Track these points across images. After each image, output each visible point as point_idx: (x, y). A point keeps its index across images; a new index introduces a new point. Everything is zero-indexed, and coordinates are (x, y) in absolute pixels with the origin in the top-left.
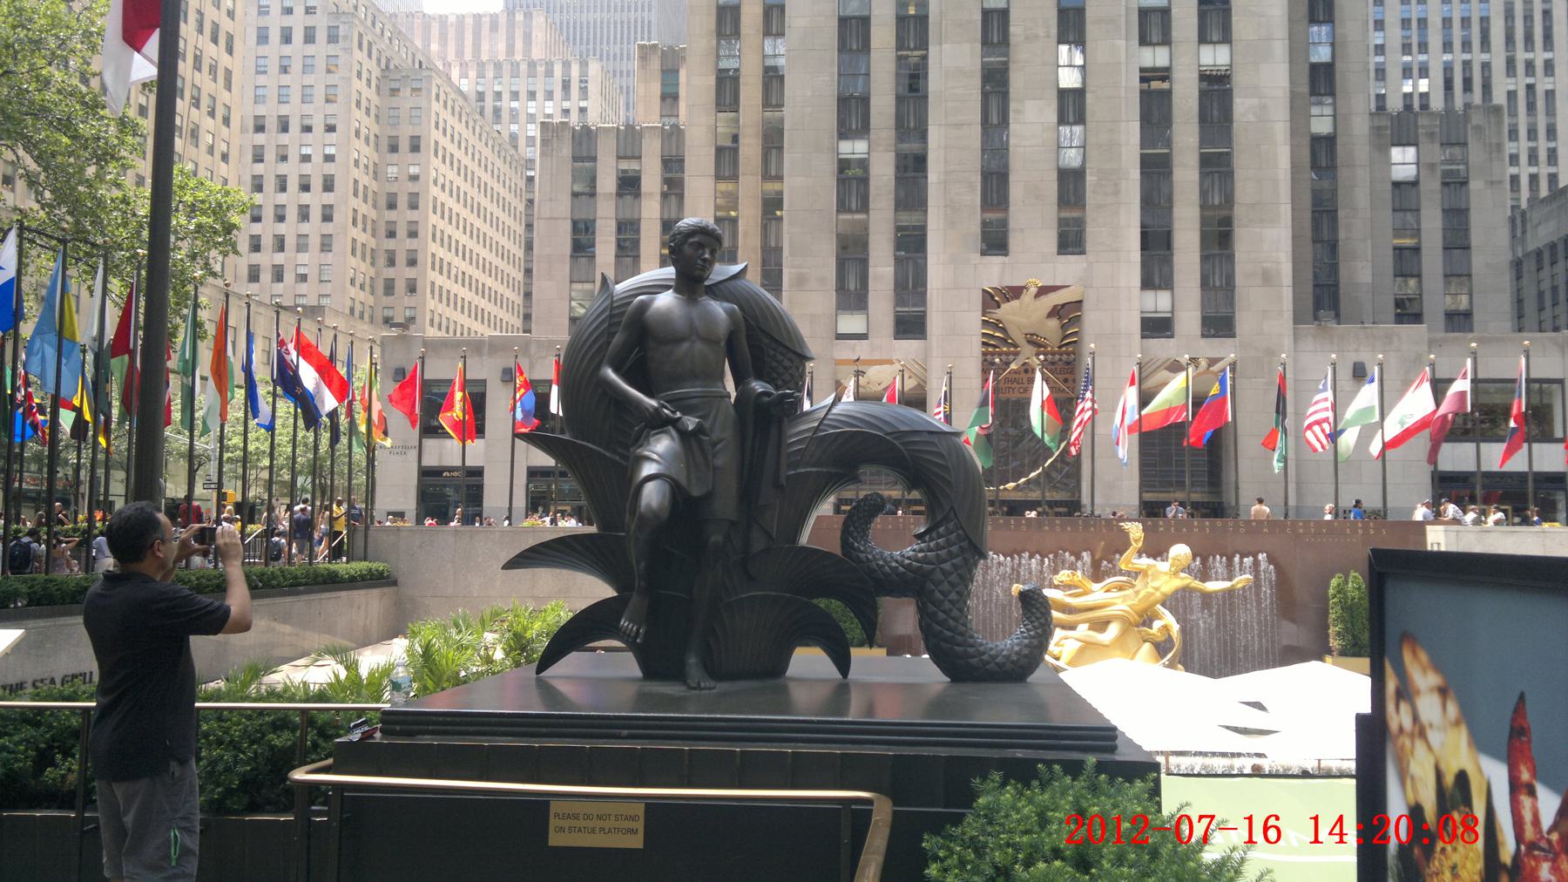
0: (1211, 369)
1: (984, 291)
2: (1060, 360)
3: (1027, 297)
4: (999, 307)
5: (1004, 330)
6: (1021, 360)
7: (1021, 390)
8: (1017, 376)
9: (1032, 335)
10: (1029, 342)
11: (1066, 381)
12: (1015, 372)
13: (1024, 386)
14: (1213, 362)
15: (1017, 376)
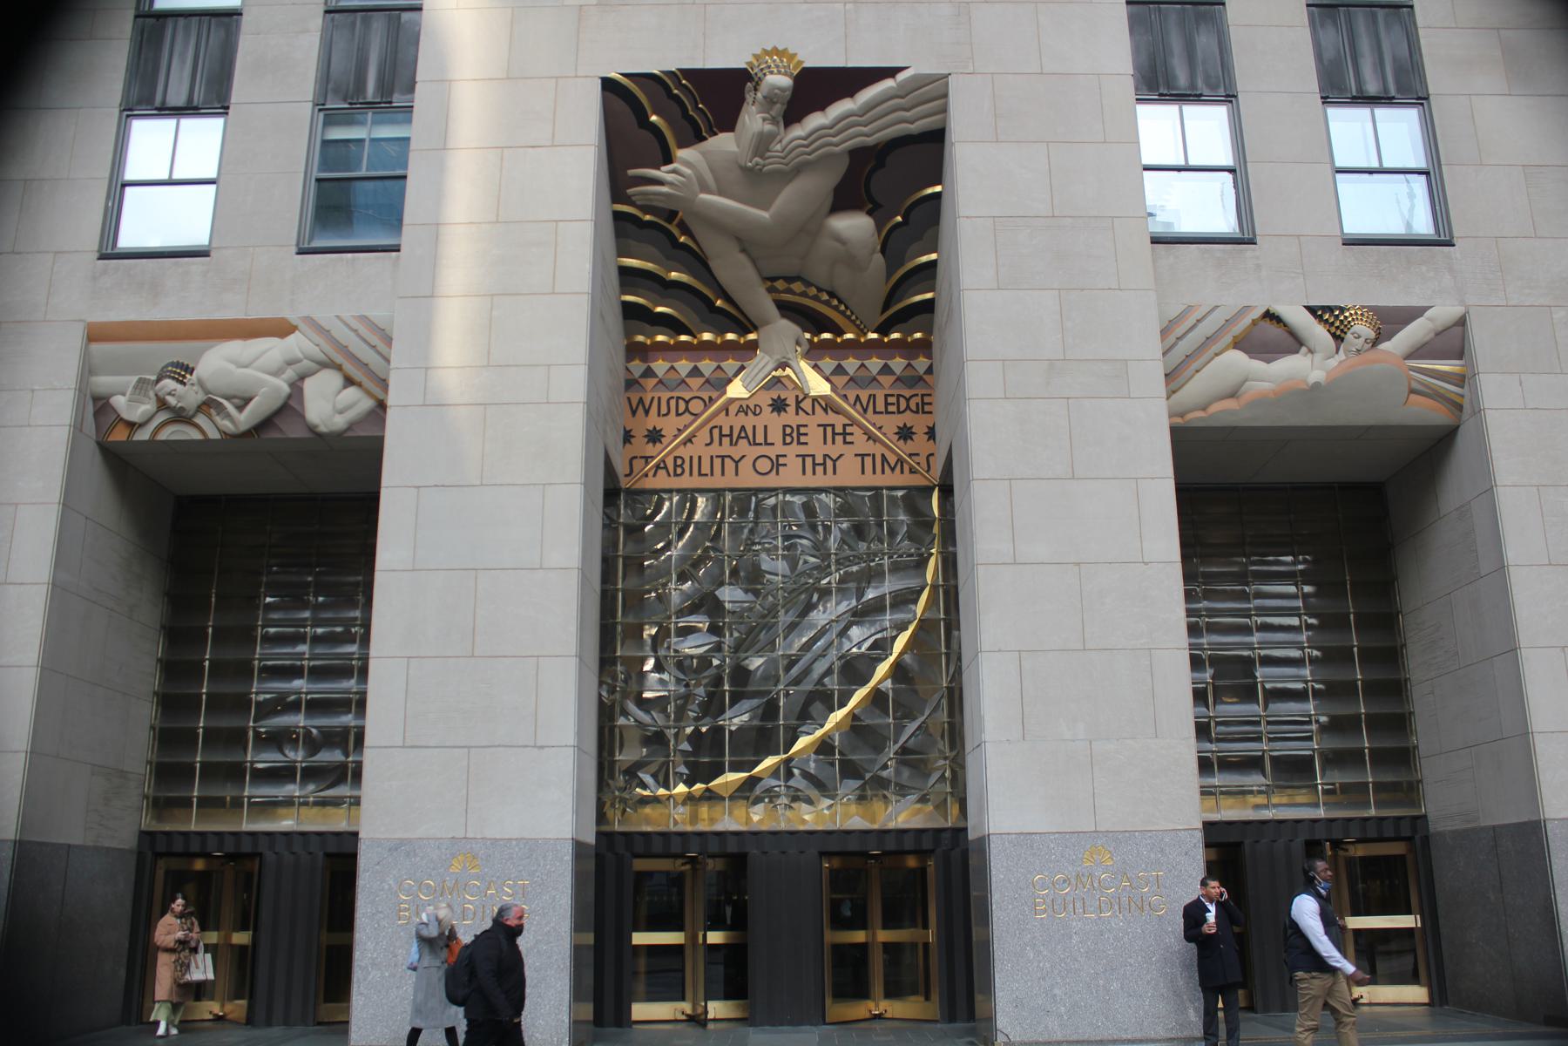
0: (1385, 346)
1: (608, 85)
2: (886, 370)
3: (753, 120)
4: (668, 159)
5: (698, 261)
6: (762, 364)
7: (764, 465)
8: (749, 421)
9: (789, 279)
10: (787, 309)
11: (905, 433)
12: (744, 408)
13: (772, 452)
14: (1389, 321)
15: (749, 421)
